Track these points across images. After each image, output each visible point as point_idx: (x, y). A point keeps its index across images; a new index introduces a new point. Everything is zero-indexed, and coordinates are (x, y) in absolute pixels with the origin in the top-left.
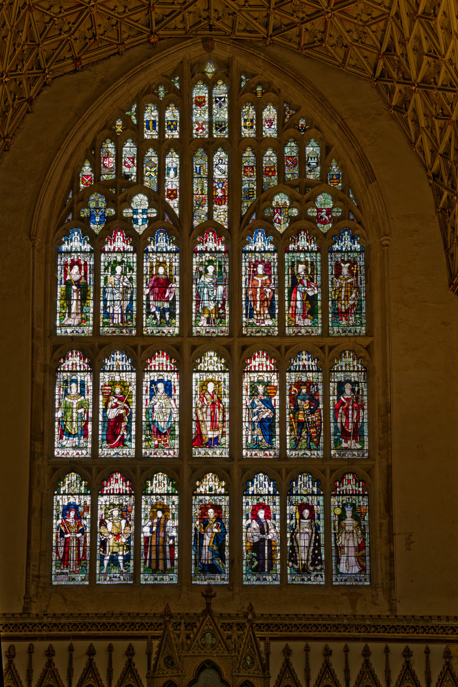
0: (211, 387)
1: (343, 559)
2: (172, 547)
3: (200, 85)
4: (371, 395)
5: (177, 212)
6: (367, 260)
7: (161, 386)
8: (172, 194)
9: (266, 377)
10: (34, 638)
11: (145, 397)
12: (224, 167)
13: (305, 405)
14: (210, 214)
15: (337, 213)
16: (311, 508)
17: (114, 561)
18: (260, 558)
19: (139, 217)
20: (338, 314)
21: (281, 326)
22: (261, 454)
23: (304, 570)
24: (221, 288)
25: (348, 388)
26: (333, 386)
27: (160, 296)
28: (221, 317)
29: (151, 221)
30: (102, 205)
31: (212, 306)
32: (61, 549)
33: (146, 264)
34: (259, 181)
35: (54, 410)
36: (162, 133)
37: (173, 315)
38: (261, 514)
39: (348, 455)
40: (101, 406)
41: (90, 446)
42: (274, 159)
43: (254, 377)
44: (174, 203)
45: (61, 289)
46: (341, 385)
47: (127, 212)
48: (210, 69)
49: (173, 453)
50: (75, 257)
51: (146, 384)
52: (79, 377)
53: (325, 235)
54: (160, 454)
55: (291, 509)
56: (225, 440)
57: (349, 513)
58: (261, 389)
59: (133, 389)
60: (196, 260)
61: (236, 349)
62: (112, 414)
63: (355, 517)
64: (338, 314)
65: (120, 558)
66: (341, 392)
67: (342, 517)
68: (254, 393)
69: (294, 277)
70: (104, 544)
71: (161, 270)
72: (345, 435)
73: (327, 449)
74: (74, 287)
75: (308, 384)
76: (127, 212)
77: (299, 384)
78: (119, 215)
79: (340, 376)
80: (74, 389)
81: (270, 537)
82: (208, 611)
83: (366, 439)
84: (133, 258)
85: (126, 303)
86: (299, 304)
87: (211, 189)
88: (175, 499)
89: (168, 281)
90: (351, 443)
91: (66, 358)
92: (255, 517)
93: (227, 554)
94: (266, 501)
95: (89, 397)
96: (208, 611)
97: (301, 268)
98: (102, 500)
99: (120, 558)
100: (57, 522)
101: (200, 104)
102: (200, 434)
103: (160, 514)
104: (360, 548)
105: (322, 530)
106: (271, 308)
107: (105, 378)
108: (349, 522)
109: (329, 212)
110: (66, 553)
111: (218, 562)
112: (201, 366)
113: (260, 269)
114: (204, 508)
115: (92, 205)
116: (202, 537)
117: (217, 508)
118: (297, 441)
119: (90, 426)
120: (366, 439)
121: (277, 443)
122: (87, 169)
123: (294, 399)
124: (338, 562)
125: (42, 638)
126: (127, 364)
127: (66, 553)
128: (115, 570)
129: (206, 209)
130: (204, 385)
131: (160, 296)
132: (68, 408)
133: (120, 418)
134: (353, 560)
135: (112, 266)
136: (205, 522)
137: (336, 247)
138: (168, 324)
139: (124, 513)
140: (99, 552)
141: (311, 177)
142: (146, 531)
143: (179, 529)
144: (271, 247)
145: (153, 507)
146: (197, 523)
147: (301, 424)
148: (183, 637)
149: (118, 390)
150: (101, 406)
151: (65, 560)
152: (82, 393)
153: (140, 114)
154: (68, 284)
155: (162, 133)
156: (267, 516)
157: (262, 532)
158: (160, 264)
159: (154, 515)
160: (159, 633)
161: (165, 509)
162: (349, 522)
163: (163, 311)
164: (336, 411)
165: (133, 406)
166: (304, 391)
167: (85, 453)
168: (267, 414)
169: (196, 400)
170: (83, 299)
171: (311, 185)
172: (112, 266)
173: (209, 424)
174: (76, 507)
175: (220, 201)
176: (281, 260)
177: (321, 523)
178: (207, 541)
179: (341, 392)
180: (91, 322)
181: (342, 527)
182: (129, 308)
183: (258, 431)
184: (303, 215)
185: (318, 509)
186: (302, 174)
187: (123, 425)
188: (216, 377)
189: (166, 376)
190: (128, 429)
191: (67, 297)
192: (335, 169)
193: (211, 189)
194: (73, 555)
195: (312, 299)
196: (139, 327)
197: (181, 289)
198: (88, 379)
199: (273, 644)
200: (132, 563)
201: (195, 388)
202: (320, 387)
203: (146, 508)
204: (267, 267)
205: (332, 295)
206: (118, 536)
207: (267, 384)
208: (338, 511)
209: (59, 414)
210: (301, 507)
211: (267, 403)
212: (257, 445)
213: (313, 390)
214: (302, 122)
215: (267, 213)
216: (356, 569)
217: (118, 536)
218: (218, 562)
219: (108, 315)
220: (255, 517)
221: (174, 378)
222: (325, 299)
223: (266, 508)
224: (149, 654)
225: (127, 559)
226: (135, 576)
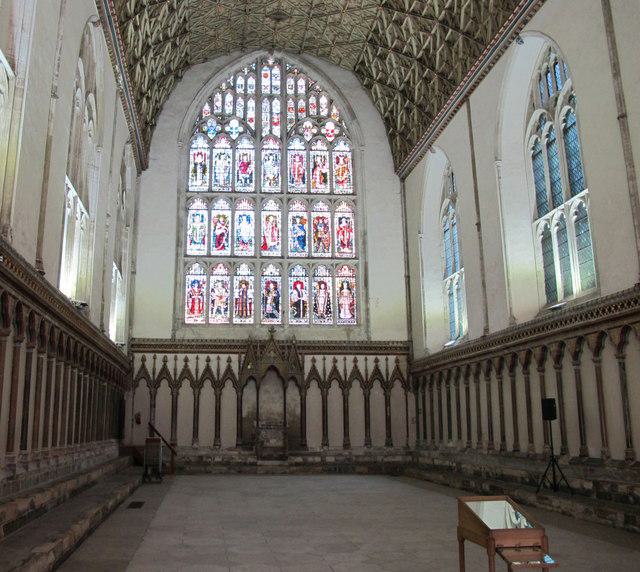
0: (271, 219)
1: (342, 311)
2: (250, 304)
3: (265, 68)
4: (356, 224)
5: (253, 128)
6: (353, 156)
7: (244, 218)
8: (251, 120)
9: (301, 214)
10: (177, 352)
11: (236, 223)
12: (279, 108)
13: (321, 229)
14: (271, 131)
15: (337, 132)
16: (325, 284)
17: (219, 311)
18: (298, 310)
19: (234, 131)
20: (338, 182)
21: (309, 188)
22: (298, 255)
23: (322, 317)
24: (277, 168)
25: (344, 220)
26: (336, 220)
27: (244, 171)
28: (277, 183)
29: (240, 134)
30: (214, 124)
31: (271, 177)
32: (190, 305)
33: (237, 155)
34: (297, 115)
35: (186, 230)
36: (245, 90)
37: (251, 181)
38: (299, 286)
39: (345, 256)
40: (213, 228)
41: (206, 249)
42: (304, 104)
43: (295, 214)
44: (252, 125)
45: (192, 166)
46: (340, 219)
47: (227, 129)
48: (271, 62)
49: (252, 254)
50: (200, 151)
51: (237, 217)
52: (201, 212)
53: (331, 143)
54: (244, 254)
55: (315, 284)
56: (279, 247)
57: (345, 285)
58: (298, 220)
59: (229, 219)
60: (264, 153)
61: (285, 200)
62: (218, 232)
63: (348, 288)
64: (338, 182)
65: (222, 310)
66: (340, 223)
67: (342, 288)
68: (294, 222)
69: (315, 163)
70: (213, 302)
71: (245, 158)
72: (343, 245)
73: (333, 252)
74: (199, 166)
75: (323, 218)
76: (227, 129)
77: (318, 218)
78: (222, 131)
79: (340, 215)
80: (198, 219)
81: (302, 299)
82: (272, 339)
83: (354, 247)
84: (230, 152)
85: (226, 175)
86: (318, 177)
87: (272, 118)
88: (252, 278)
89: (249, 164)
90: (346, 250)
91: (194, 202)
92: (296, 288)
93: (280, 308)
94: (302, 279)
95: (206, 223)
96: (272, 339)
97: (319, 158)
98: (213, 279)
99: (222, 310)
100: (187, 290)
101: (266, 77)
102: (265, 244)
103: (244, 286)
104: (351, 305)
105: (331, 295)
106: (303, 179)
107: (214, 213)
108: (345, 291)
109: (332, 131)
110: (193, 306)
111: (275, 312)
112: (266, 208)
113: (297, 159)
114: (268, 283)
115: (209, 124)
116: (266, 299)
117: (275, 283)
118: (317, 248)
119: (206, 239)
120: (354, 247)
121: (306, 248)
122: (207, 107)
123: (315, 226)
124: (340, 312)
125: (182, 352)
126: (227, 206)
127: (193, 306)
128: (219, 316)
129: (268, 128)
130: (267, 218)
131: (244, 171)
132: (194, 229)
133: (222, 235)
134: (348, 311)
135: (219, 156)
136: (268, 291)
137: (336, 149)
138: (249, 185)
139: (224, 285)
140: (211, 306)
141: (322, 114)
142: (236, 296)
143: (254, 294)
144: (303, 148)
145: (240, 282)
146: (264, 291)
147: (319, 239)
148: (258, 353)
149: (221, 220)
150: (213, 228)
151: (192, 310)
152: (202, 221)
153: (235, 81)
154: (196, 164)
155: (245, 90)
156: (302, 288)
157: (299, 296)
158: (244, 155)
159: (240, 287)
160: (245, 350)
161: (247, 284)
162: (345, 291)
163: (246, 179)
164: (338, 232)
165: (230, 228)
166: (321, 221)
167: (204, 253)
168: (302, 233)
169: (263, 226)
170: (204, 172)
171: (324, 118)
172: (219, 156)
173: (270, 238)
174: (198, 282)
175: (276, 124)
176: (308, 155)
177: (331, 291)
178: (269, 301)
179: (340, 223)
180: (208, 184)
181: (341, 294)
182: (228, 177)
183: (297, 242)
184: (319, 133)
185: (330, 284)
186: (318, 113)
187: (225, 238)
188: (274, 214)
189: (247, 213)
190: (227, 240)
191: (195, 171)
192: (335, 111)
193: (272, 118)
194: (196, 308)
195: (324, 175)
196: (233, 187)
197: (256, 168)
198: (206, 214)
199: (306, 357)
200: (228, 312)
201: (263, 219)
202: (329, 219)
203: (236, 283)
204: (301, 158)
205: (335, 173)
206: (221, 297)
207: (301, 218)
208: (340, 286)
209: (189, 232)
210: (320, 283)
211: (302, 228)
212: (296, 249)
213: (326, 222)
214: (318, 87)
215: (301, 131)
216: (350, 316)
217: (221, 297)
218: (275, 312)
219: (216, 181)
220: (296, 288)
221: (252, 214)
222: (331, 174)
223: (301, 283)
224: (239, 362)
225: (226, 310)
226: (231, 319)
